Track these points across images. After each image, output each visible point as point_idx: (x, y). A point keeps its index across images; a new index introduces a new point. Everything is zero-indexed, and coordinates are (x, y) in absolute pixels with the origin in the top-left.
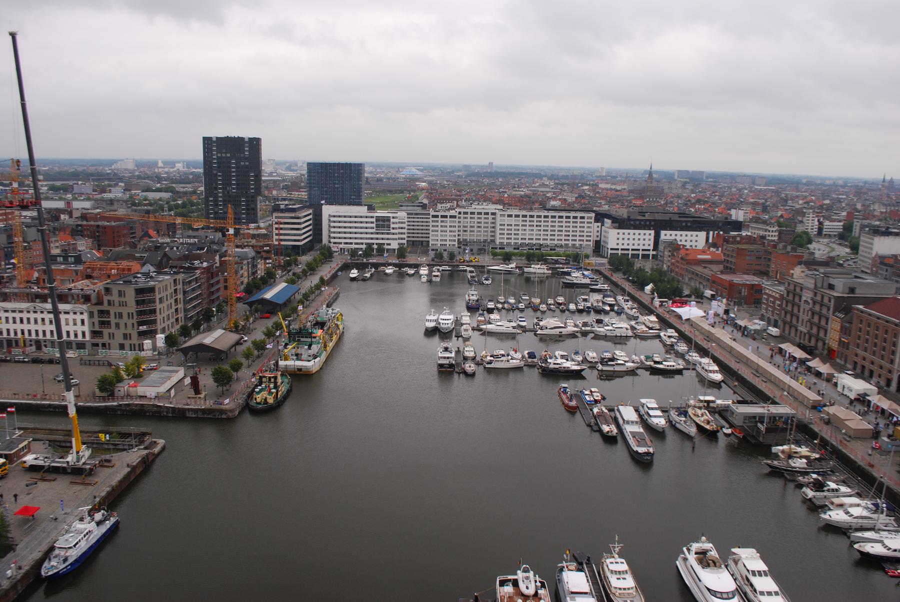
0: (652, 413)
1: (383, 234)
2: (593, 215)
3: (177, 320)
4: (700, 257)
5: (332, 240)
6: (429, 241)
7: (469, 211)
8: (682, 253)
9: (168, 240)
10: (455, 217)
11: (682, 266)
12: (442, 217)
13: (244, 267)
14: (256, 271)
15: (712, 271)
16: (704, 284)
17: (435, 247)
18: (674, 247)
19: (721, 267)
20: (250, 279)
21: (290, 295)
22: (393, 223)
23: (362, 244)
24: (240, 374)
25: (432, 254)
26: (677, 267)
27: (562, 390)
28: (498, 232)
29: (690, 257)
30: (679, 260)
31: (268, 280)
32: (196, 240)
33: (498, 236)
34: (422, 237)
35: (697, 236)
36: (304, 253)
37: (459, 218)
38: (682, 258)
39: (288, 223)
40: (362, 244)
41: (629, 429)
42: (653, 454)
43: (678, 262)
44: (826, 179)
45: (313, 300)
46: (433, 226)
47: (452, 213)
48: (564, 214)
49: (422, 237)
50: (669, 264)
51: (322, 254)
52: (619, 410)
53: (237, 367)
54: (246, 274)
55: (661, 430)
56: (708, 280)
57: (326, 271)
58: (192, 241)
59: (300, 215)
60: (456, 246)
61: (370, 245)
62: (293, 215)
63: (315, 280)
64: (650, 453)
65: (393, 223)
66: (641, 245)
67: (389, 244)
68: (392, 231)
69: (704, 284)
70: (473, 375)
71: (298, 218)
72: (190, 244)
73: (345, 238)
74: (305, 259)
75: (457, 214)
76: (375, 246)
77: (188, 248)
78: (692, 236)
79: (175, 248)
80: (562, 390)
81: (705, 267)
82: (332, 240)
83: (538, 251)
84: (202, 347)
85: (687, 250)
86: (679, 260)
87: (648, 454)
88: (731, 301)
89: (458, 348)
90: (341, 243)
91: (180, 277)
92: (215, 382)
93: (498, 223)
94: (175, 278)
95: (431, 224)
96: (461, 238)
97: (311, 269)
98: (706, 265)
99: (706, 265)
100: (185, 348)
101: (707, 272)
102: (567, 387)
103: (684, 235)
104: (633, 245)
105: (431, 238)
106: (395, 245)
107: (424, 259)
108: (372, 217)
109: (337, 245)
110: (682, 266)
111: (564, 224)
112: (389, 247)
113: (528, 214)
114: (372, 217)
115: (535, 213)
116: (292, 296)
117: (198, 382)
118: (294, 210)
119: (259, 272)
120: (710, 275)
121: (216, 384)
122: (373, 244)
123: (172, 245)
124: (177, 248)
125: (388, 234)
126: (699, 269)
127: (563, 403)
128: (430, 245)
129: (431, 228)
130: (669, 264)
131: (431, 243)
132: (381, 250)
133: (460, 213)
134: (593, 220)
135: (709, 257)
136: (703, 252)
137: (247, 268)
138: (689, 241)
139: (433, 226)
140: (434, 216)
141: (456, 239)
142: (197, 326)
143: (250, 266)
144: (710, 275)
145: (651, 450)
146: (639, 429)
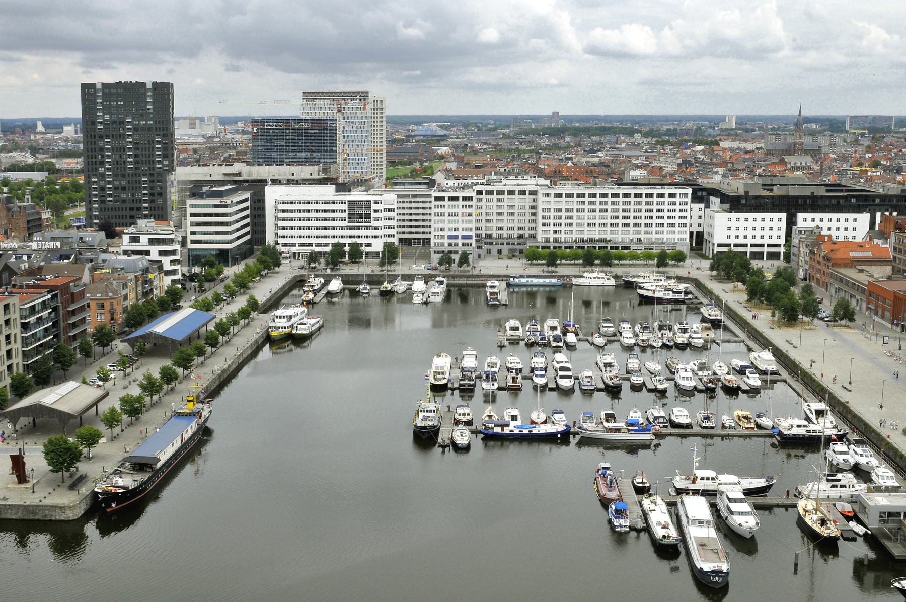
0: (734, 507)
1: (359, 228)
2: (689, 191)
3: (10, 368)
4: (852, 254)
5: (281, 240)
6: (430, 239)
7: (494, 188)
8: (825, 250)
9: (15, 244)
10: (470, 199)
11: (825, 269)
12: (451, 199)
13: (129, 284)
14: (151, 290)
15: (872, 276)
16: (858, 297)
17: (440, 248)
18: (816, 238)
19: (888, 270)
20: (140, 302)
21: (197, 326)
22: (375, 211)
23: (326, 245)
24: (94, 450)
25: (435, 258)
26: (819, 271)
27: (600, 472)
28: (540, 221)
29: (839, 255)
30: (821, 260)
31: (171, 302)
32: (58, 244)
33: (540, 228)
34: (410, 233)
35: (855, 220)
36: (235, 262)
37: (478, 200)
38: (824, 257)
39: (210, 215)
40: (326, 245)
41: (694, 533)
42: (727, 573)
43: (819, 263)
44: (681, 119)
45: (235, 335)
46: (437, 214)
47: (467, 193)
48: (644, 191)
49: (410, 233)
50: (807, 267)
51: (261, 262)
52: (682, 502)
53: (92, 439)
54: (132, 296)
55: (749, 536)
56: (863, 291)
57: (263, 291)
58: (52, 245)
59: (229, 202)
60: (474, 245)
61: (338, 247)
62: (217, 201)
63: (241, 302)
64: (722, 572)
65: (375, 211)
66: (749, 237)
67: (369, 245)
68: (374, 224)
69: (858, 297)
70: (467, 449)
71: (226, 206)
72: (50, 251)
73: (300, 237)
74: (231, 271)
75: (473, 194)
76: (347, 249)
77: (46, 255)
78: (822, 220)
79: (25, 258)
80: (600, 472)
81: (861, 271)
82: (281, 240)
83: (568, 250)
84: (38, 410)
85: (835, 243)
86: (821, 260)
87: (717, 573)
88: (897, 325)
89: (449, 407)
90: (293, 245)
91: (14, 300)
92: (49, 464)
93: (540, 207)
94: (5, 302)
95: (433, 211)
96: (483, 232)
97: (242, 284)
98: (863, 268)
99: (863, 268)
100: (13, 411)
101: (863, 278)
102: (607, 468)
103: (759, 220)
104: (737, 237)
105: (433, 234)
106: (377, 246)
107: (420, 268)
108: (342, 203)
109: (288, 248)
110: (825, 269)
111: (632, 207)
112: (368, 249)
113: (587, 191)
114: (342, 203)
115: (598, 191)
116: (200, 328)
117: (24, 464)
118: (219, 194)
119: (155, 292)
120: (867, 283)
121: (51, 468)
122: (345, 245)
123: (19, 252)
124: (29, 257)
125: (367, 228)
126: (851, 274)
127: (598, 491)
128: (433, 245)
129: (433, 218)
130: (807, 267)
131: (433, 241)
132: (356, 254)
133: (480, 193)
134: (689, 199)
135: (869, 254)
136: (861, 246)
137: (134, 286)
138: (834, 229)
139: (437, 214)
140: (437, 199)
141: (473, 233)
142: (44, 379)
143: (140, 282)
144: (867, 283)
145: (725, 567)
146: (711, 533)
